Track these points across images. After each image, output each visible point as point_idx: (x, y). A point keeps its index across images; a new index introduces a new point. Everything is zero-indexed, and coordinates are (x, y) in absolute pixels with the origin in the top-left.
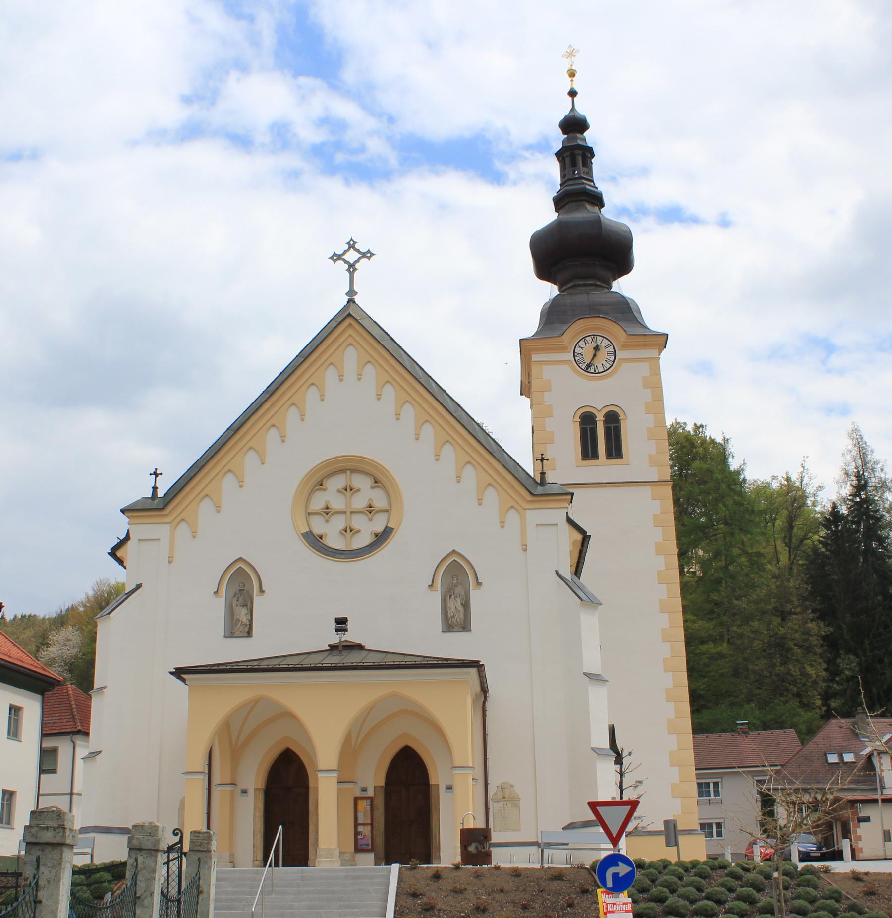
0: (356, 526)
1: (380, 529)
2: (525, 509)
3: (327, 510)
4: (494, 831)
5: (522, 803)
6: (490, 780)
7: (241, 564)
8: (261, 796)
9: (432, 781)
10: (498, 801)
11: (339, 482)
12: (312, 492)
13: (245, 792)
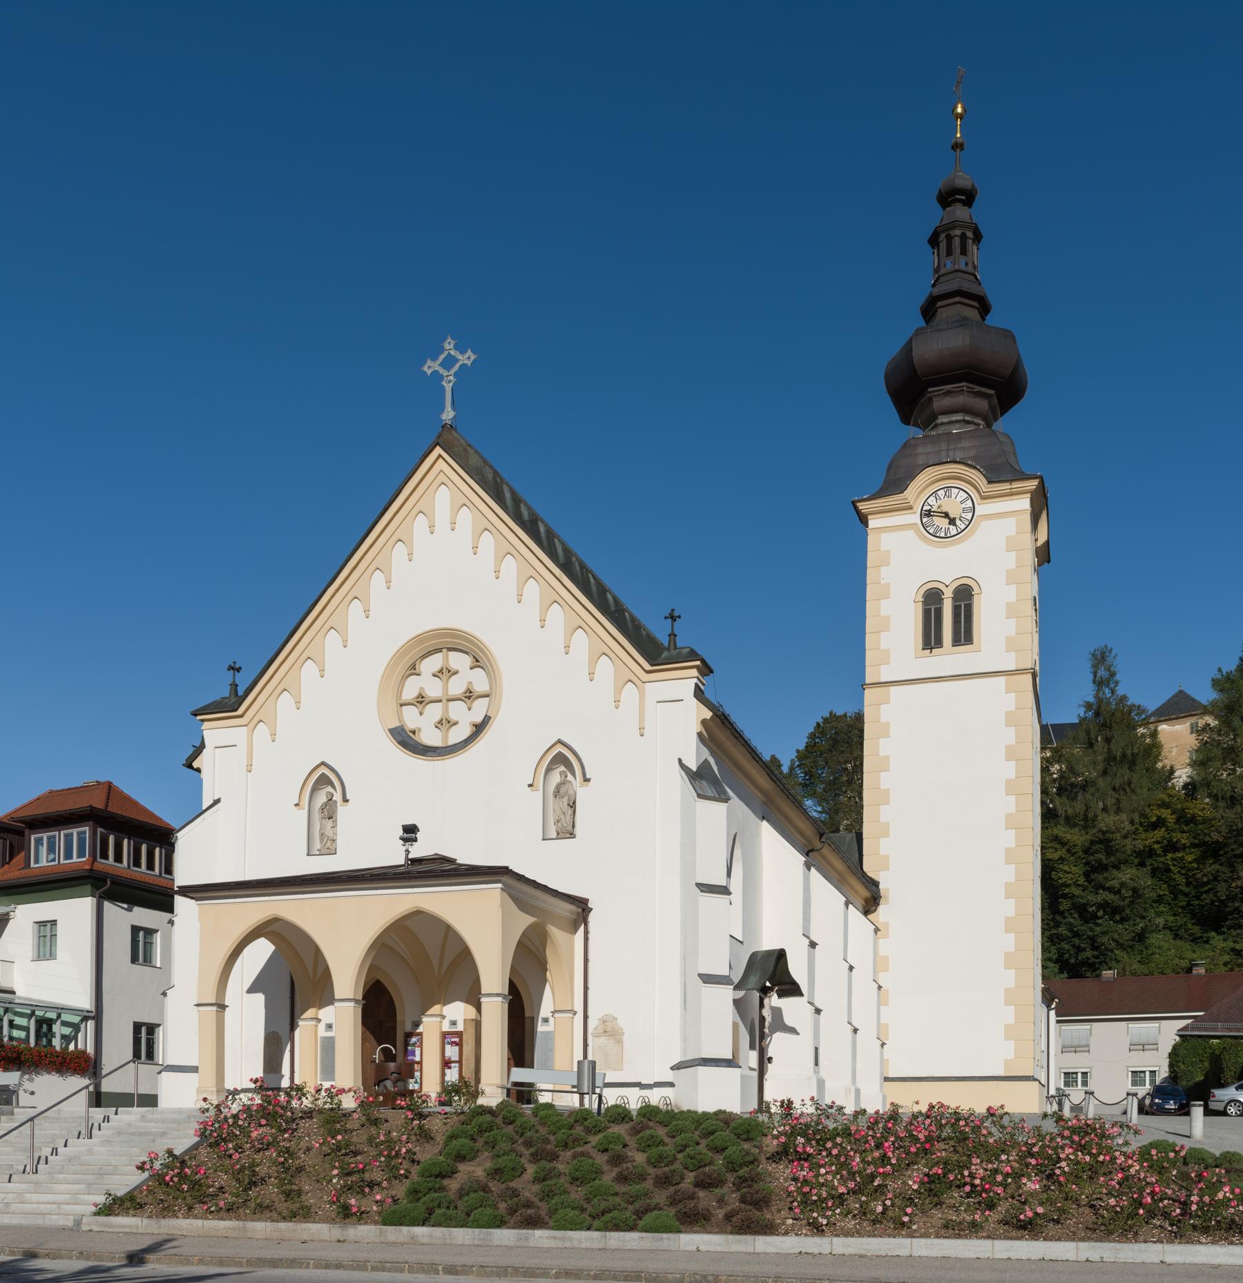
1: (479, 720)
6: (590, 1013)
7: (323, 770)
10: (599, 1036)
11: (435, 662)
12: (405, 677)
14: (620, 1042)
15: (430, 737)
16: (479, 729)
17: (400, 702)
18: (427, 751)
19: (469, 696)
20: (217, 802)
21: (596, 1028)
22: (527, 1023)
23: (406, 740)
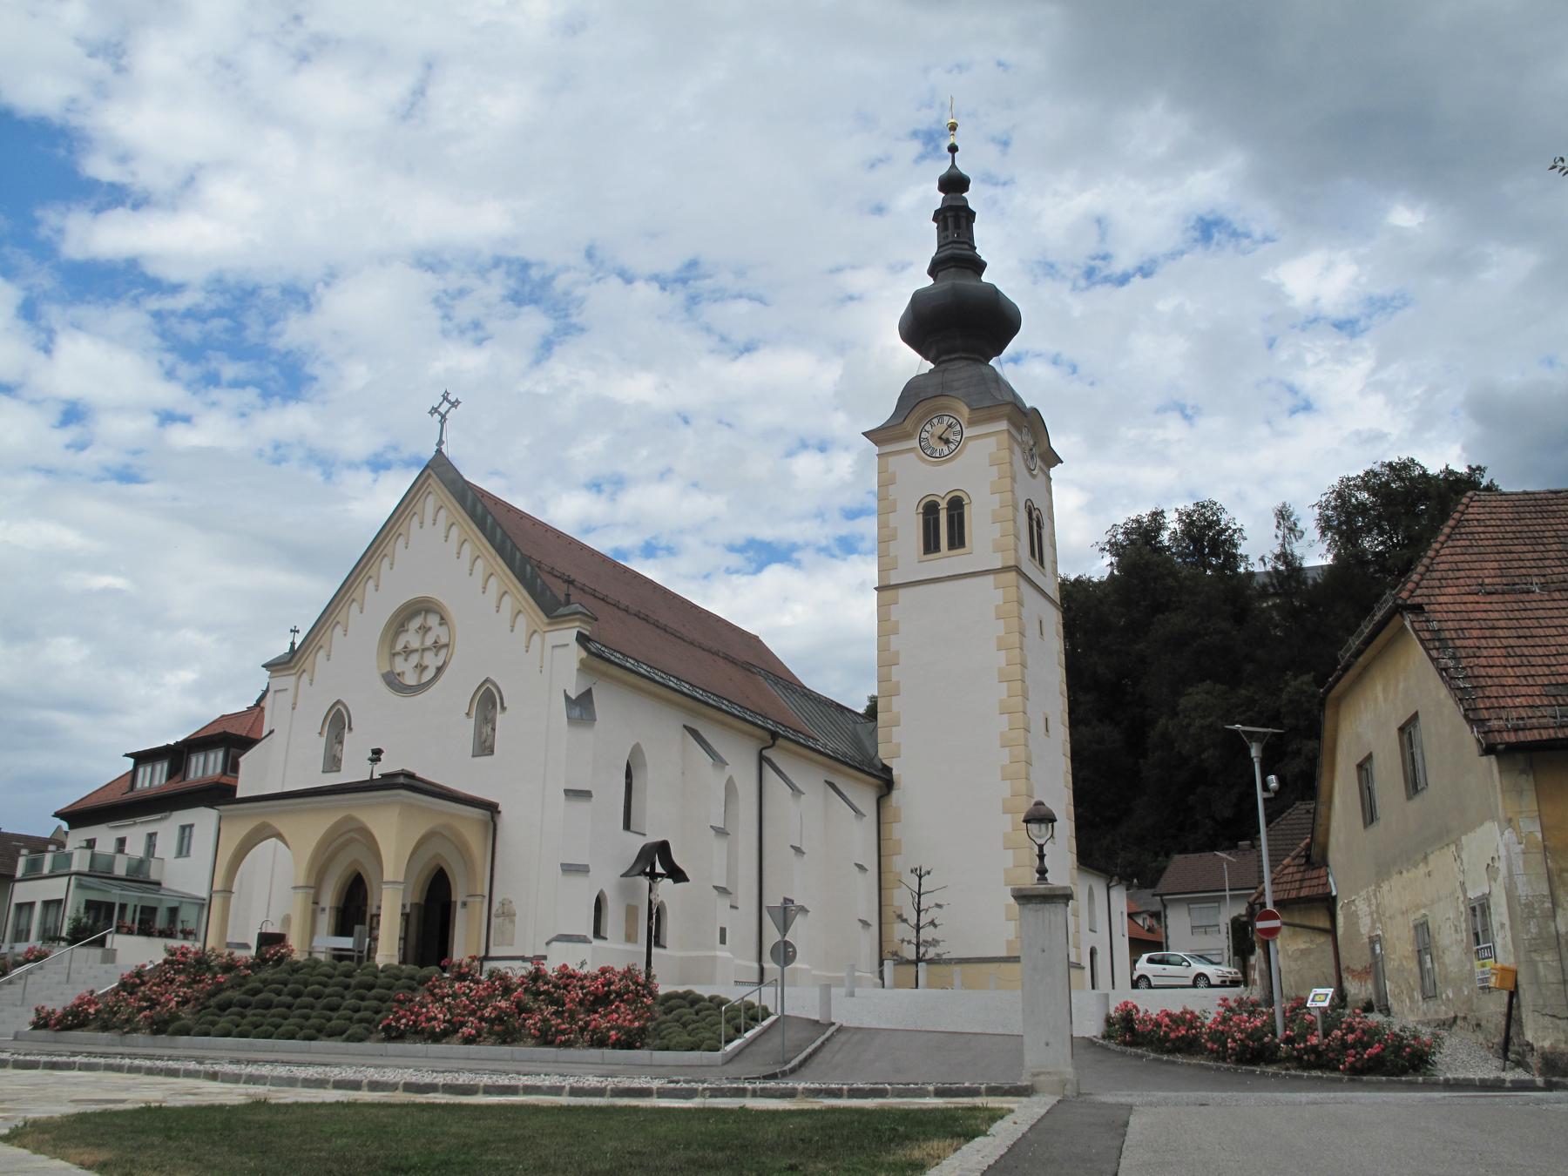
0: (426, 662)
1: (440, 664)
2: (545, 632)
3: (407, 652)
4: (494, 945)
5: (517, 919)
8: (333, 913)
9: (453, 899)
11: (415, 624)
12: (397, 635)
13: (323, 910)
14: (512, 922)
15: (411, 679)
16: (439, 670)
17: (393, 651)
18: (405, 689)
19: (437, 647)
20: (271, 732)
21: (497, 910)
22: (453, 904)
23: (393, 682)
